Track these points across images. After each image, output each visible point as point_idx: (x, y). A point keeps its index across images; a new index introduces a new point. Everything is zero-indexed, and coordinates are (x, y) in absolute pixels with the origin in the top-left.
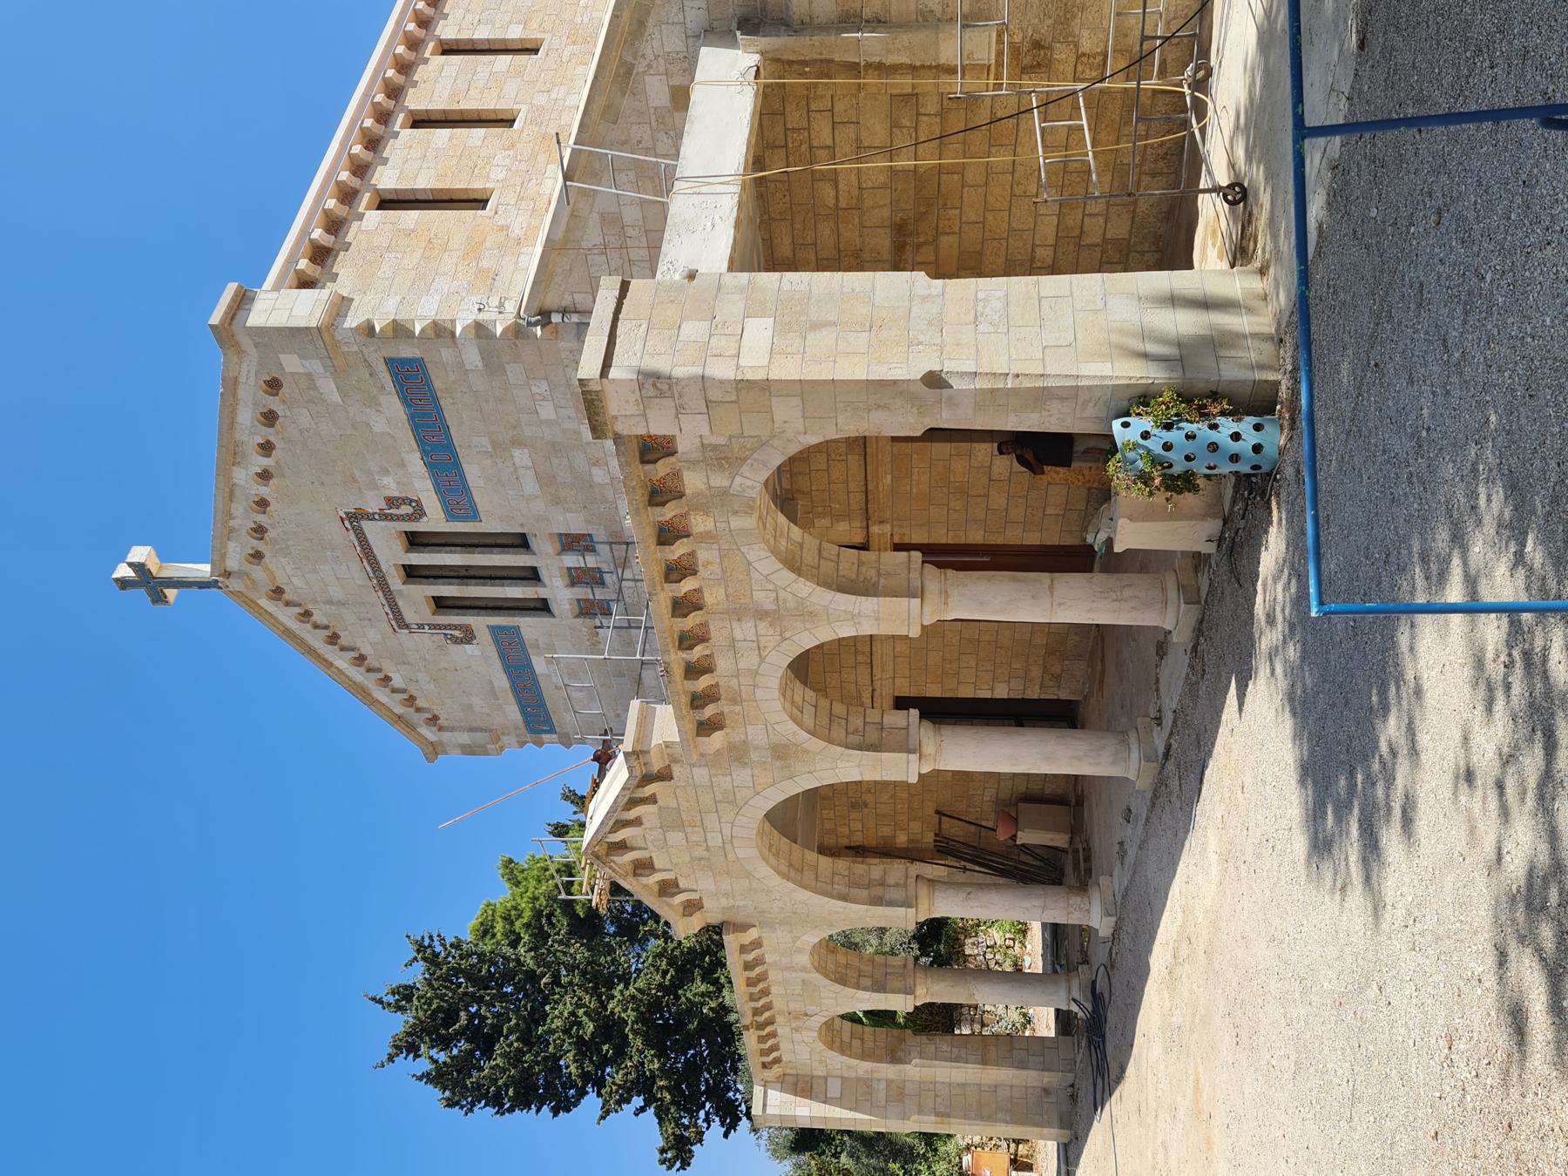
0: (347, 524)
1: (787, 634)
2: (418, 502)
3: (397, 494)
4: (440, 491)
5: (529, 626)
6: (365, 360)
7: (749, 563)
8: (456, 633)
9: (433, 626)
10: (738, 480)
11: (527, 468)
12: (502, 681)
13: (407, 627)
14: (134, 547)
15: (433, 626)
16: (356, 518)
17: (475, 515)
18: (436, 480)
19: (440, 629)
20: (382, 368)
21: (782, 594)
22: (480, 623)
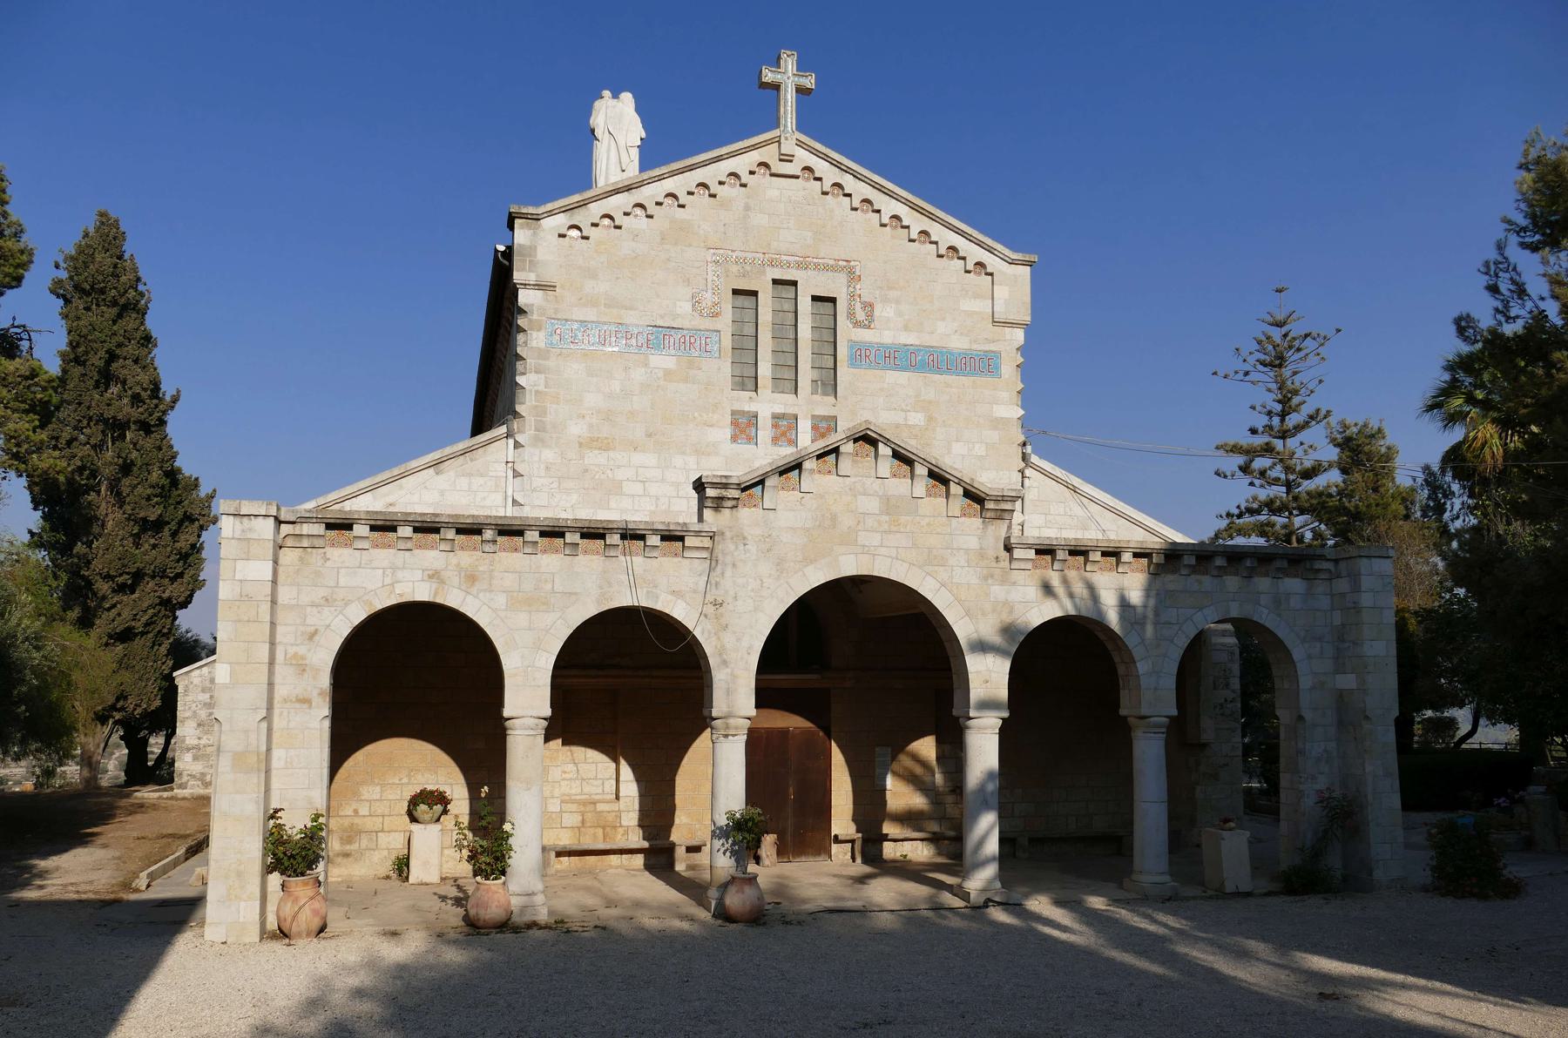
1: (1136, 627)
2: (869, 327)
3: (877, 313)
4: (880, 347)
5: (722, 369)
6: (998, 340)
7: (1201, 609)
10: (1266, 611)
11: (906, 419)
21: (1176, 627)
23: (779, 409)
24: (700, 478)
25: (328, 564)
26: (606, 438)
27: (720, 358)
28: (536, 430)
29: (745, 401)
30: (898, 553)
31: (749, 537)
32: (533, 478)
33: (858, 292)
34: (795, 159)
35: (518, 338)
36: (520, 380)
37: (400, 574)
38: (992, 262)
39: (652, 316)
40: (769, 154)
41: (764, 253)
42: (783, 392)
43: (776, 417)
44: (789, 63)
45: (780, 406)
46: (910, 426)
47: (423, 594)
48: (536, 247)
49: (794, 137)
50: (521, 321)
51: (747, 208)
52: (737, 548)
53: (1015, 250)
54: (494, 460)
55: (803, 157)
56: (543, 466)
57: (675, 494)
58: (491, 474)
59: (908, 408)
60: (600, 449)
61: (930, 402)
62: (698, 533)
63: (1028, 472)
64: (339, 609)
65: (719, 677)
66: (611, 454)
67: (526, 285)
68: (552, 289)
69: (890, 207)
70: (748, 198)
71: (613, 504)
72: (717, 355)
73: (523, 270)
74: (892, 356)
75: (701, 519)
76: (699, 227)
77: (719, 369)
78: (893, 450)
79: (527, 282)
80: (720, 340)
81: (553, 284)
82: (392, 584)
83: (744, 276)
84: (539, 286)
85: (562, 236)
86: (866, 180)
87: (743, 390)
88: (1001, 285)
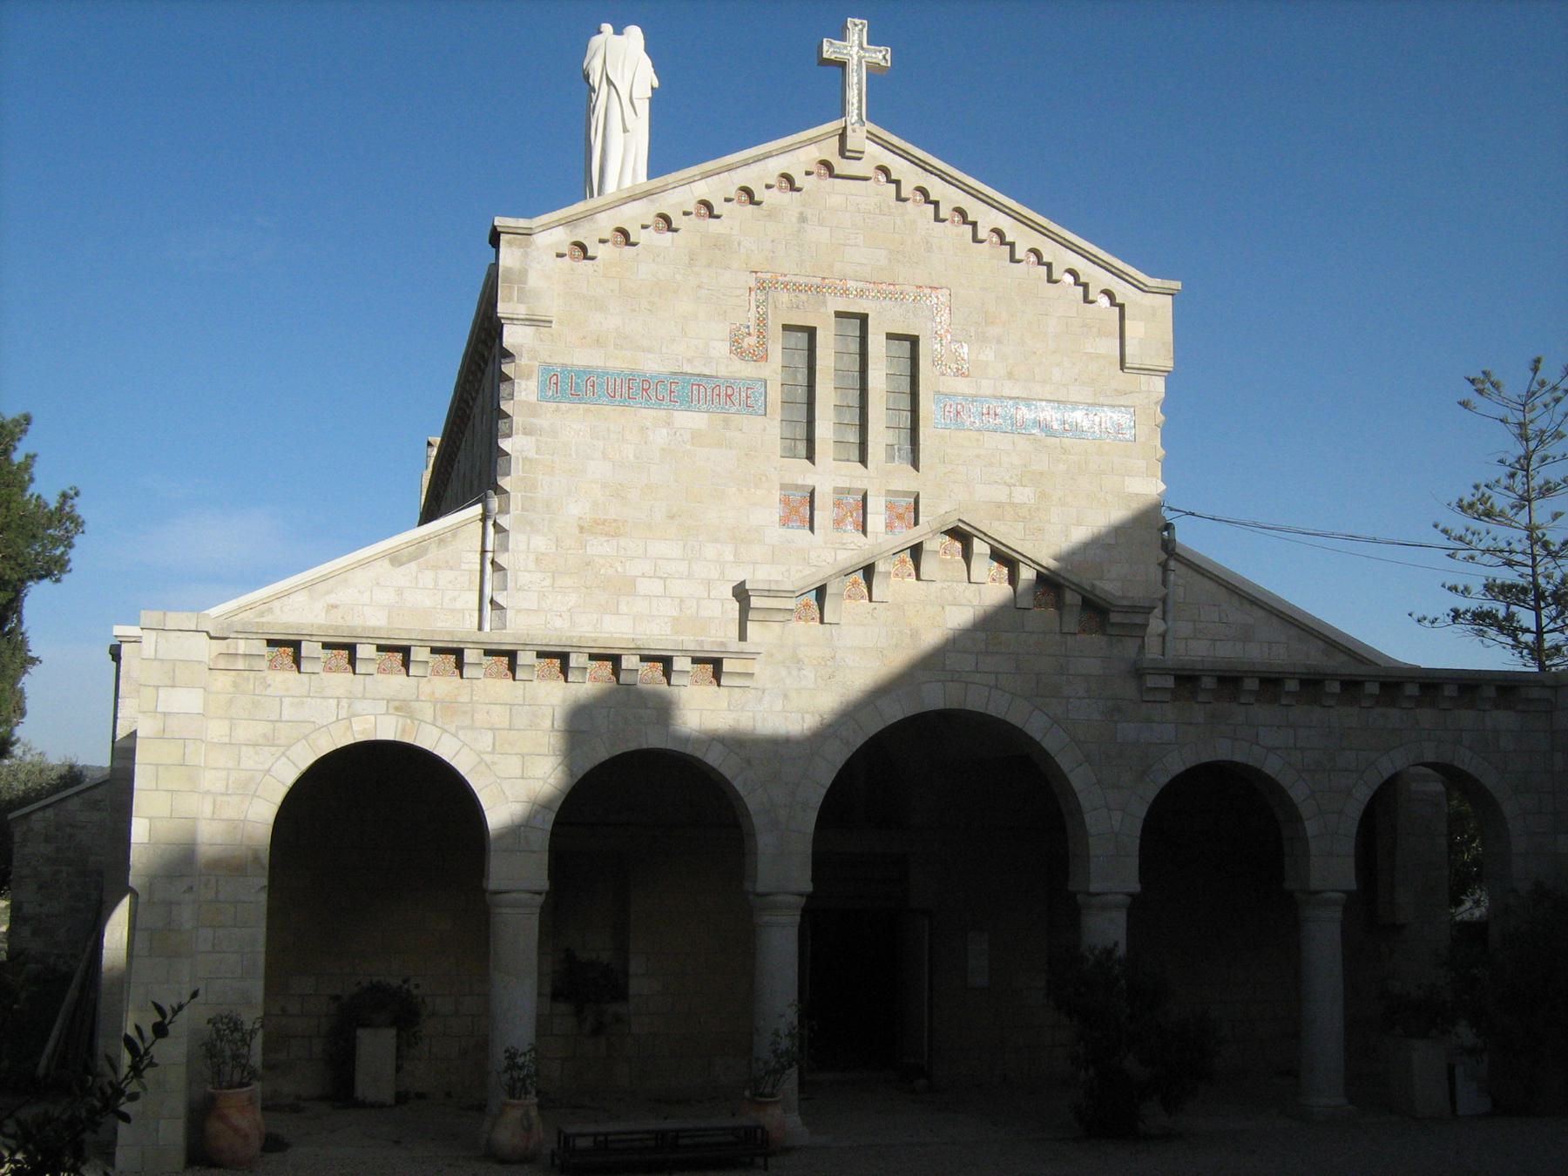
5: (769, 430)
6: (1131, 392)
8: (752, 341)
12: (652, 365)
15: (762, 321)
23: (844, 483)
24: (743, 583)
25: (269, 692)
26: (615, 521)
27: (765, 415)
28: (523, 509)
29: (801, 473)
30: (997, 679)
31: (806, 660)
32: (520, 573)
34: (865, 156)
35: (501, 388)
36: (505, 444)
37: (359, 706)
38: (1123, 291)
39: (677, 360)
41: (824, 278)
42: (848, 460)
43: (840, 491)
44: (857, 29)
45: (843, 478)
46: (1015, 505)
47: (388, 731)
48: (527, 271)
49: (865, 129)
50: (507, 368)
51: (803, 219)
52: (790, 673)
54: (468, 548)
55: (876, 154)
56: (532, 557)
57: (706, 596)
58: (464, 566)
60: (607, 534)
61: (1042, 474)
62: (740, 655)
63: (1172, 564)
64: (283, 749)
65: (765, 842)
66: (623, 542)
67: (512, 319)
68: (549, 325)
69: (988, 218)
70: (804, 206)
71: (623, 608)
72: (762, 412)
73: (510, 300)
74: (992, 412)
75: (743, 636)
76: (739, 244)
77: (764, 430)
78: (992, 547)
79: (515, 316)
80: (766, 392)
81: (547, 319)
82: (349, 718)
83: (797, 307)
84: (532, 321)
85: (560, 255)
86: (957, 183)
87: (795, 457)
88: (1134, 319)
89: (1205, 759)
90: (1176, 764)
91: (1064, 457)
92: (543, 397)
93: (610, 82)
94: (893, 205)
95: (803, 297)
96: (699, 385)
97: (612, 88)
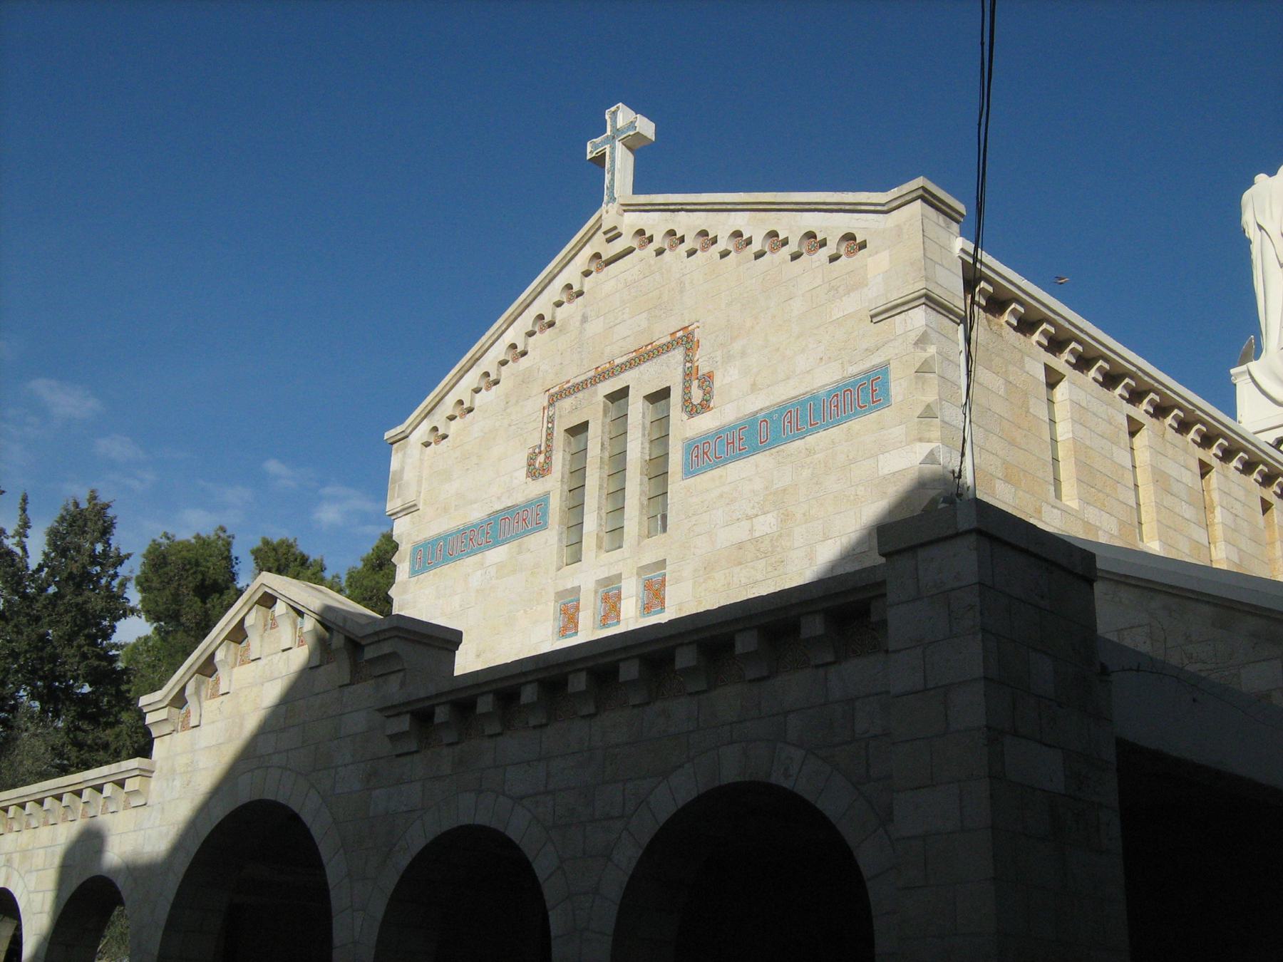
0: (680, 334)
3: (717, 383)
4: (718, 434)
5: (548, 542)
8: (541, 458)
9: (550, 434)
11: (751, 530)
12: (476, 514)
13: (551, 404)
14: (654, 125)
15: (550, 434)
16: (686, 341)
17: (691, 473)
18: (734, 427)
19: (547, 440)
20: (876, 360)
22: (554, 485)
33: (696, 364)
40: (598, 244)
46: (756, 540)
53: (884, 188)
59: (755, 512)
68: (415, 509)
88: (877, 253)
89: (447, 825)
90: (417, 838)
91: (808, 460)
92: (414, 572)
93: (1261, 228)
94: (653, 262)
95: (580, 395)
96: (505, 519)
97: (1262, 231)
